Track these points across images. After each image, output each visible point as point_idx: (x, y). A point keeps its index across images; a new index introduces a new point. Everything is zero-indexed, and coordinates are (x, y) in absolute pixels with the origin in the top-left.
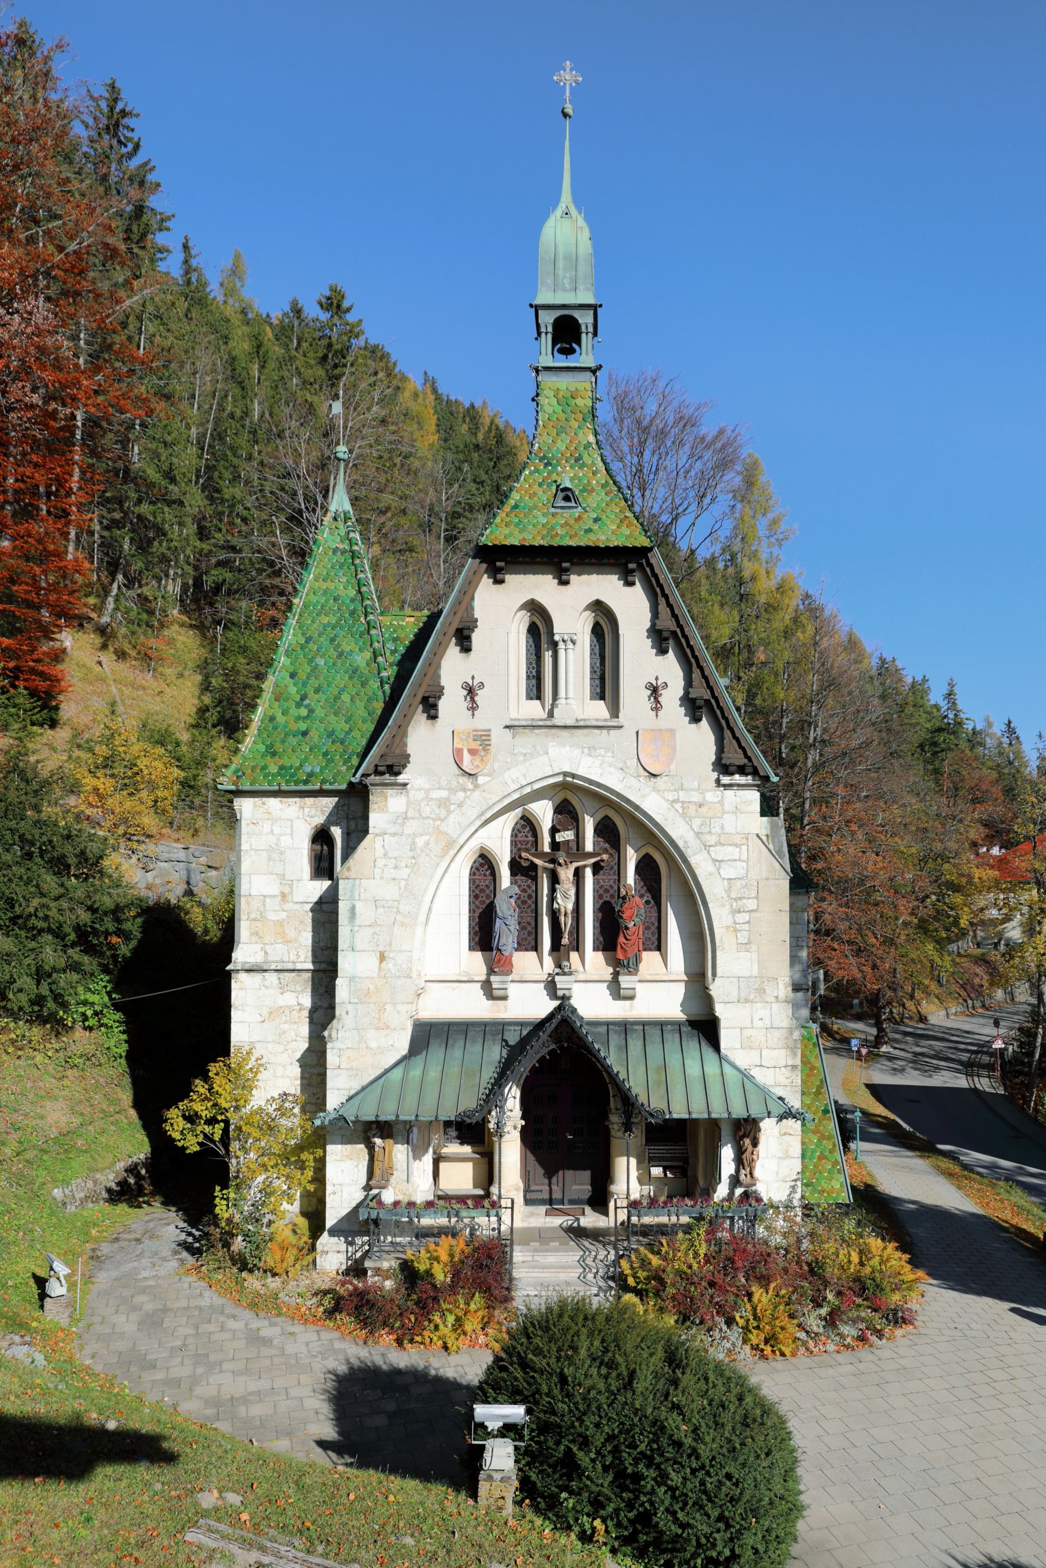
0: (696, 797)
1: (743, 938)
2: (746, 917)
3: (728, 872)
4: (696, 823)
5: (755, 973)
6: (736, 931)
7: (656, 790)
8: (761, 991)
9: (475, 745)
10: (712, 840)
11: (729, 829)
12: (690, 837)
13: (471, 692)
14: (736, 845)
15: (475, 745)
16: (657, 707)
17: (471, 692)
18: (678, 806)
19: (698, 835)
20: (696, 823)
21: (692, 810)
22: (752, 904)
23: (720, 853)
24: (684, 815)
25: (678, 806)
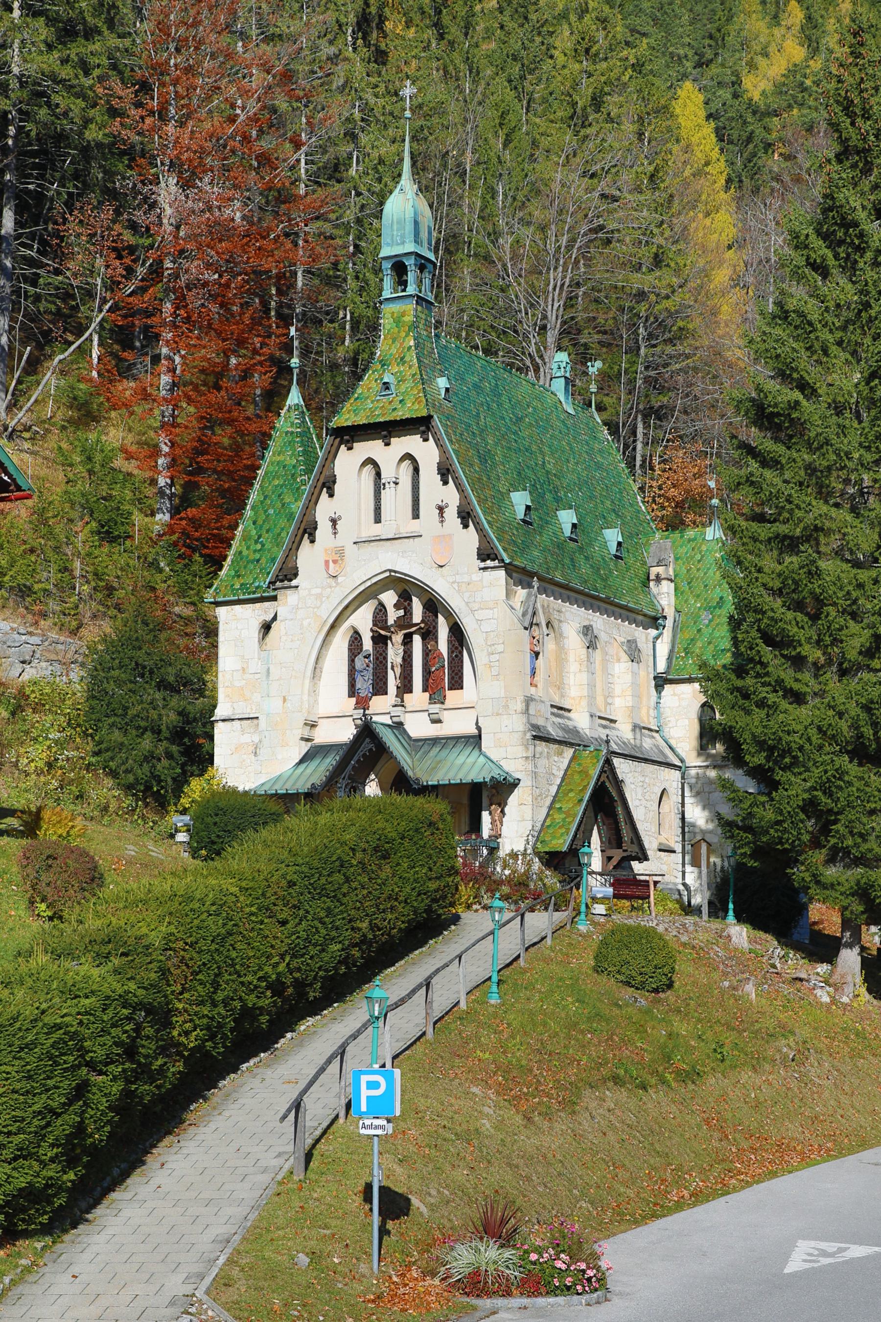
0: (466, 579)
1: (495, 671)
2: (497, 657)
3: (486, 627)
4: (467, 595)
5: (503, 695)
6: (490, 667)
8: (506, 707)
10: (475, 606)
13: (334, 522)
15: (336, 557)
17: (334, 522)
18: (455, 586)
19: (467, 603)
20: (467, 595)
22: (500, 648)
23: (480, 615)
24: (459, 591)
25: (455, 586)
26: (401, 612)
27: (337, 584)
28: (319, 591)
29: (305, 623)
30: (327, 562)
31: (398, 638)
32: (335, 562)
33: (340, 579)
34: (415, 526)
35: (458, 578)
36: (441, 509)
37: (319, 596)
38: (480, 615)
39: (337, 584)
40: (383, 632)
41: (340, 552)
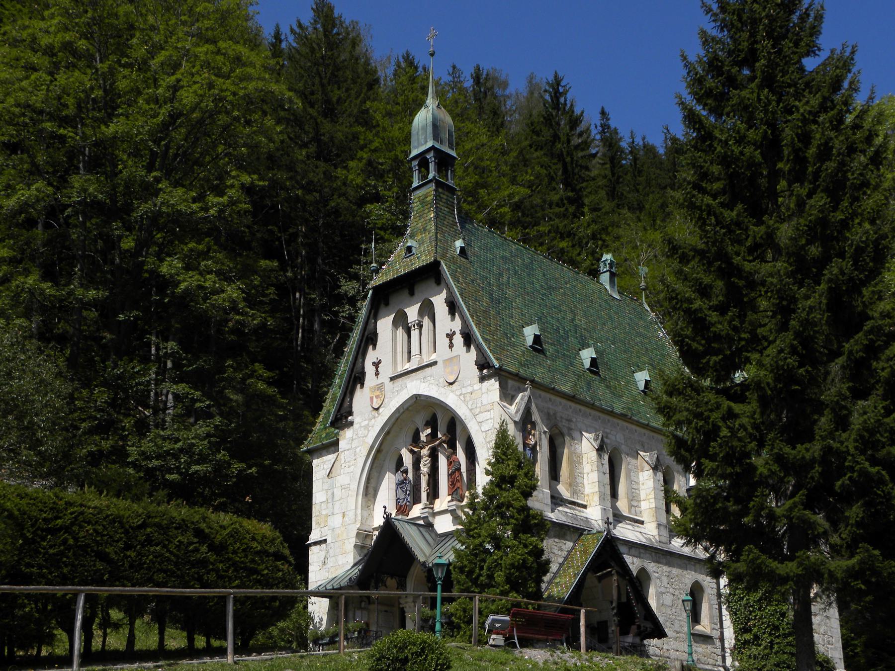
0: (470, 389)
3: (485, 427)
4: (470, 403)
7: (452, 392)
9: (378, 393)
11: (485, 402)
12: (468, 413)
13: (377, 364)
14: (488, 411)
16: (451, 346)
18: (462, 397)
20: (470, 403)
21: (468, 398)
26: (429, 431)
27: (379, 414)
28: (366, 422)
29: (358, 450)
30: (372, 399)
31: (425, 452)
32: (377, 397)
33: (381, 410)
34: (434, 357)
35: (464, 390)
36: (450, 336)
37: (367, 427)
38: (480, 418)
39: (379, 414)
40: (416, 450)
41: (380, 387)
